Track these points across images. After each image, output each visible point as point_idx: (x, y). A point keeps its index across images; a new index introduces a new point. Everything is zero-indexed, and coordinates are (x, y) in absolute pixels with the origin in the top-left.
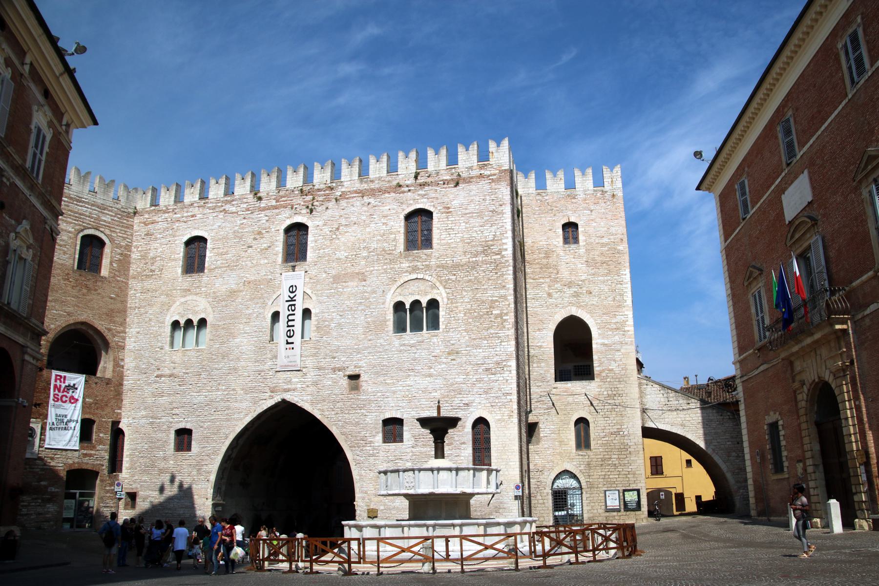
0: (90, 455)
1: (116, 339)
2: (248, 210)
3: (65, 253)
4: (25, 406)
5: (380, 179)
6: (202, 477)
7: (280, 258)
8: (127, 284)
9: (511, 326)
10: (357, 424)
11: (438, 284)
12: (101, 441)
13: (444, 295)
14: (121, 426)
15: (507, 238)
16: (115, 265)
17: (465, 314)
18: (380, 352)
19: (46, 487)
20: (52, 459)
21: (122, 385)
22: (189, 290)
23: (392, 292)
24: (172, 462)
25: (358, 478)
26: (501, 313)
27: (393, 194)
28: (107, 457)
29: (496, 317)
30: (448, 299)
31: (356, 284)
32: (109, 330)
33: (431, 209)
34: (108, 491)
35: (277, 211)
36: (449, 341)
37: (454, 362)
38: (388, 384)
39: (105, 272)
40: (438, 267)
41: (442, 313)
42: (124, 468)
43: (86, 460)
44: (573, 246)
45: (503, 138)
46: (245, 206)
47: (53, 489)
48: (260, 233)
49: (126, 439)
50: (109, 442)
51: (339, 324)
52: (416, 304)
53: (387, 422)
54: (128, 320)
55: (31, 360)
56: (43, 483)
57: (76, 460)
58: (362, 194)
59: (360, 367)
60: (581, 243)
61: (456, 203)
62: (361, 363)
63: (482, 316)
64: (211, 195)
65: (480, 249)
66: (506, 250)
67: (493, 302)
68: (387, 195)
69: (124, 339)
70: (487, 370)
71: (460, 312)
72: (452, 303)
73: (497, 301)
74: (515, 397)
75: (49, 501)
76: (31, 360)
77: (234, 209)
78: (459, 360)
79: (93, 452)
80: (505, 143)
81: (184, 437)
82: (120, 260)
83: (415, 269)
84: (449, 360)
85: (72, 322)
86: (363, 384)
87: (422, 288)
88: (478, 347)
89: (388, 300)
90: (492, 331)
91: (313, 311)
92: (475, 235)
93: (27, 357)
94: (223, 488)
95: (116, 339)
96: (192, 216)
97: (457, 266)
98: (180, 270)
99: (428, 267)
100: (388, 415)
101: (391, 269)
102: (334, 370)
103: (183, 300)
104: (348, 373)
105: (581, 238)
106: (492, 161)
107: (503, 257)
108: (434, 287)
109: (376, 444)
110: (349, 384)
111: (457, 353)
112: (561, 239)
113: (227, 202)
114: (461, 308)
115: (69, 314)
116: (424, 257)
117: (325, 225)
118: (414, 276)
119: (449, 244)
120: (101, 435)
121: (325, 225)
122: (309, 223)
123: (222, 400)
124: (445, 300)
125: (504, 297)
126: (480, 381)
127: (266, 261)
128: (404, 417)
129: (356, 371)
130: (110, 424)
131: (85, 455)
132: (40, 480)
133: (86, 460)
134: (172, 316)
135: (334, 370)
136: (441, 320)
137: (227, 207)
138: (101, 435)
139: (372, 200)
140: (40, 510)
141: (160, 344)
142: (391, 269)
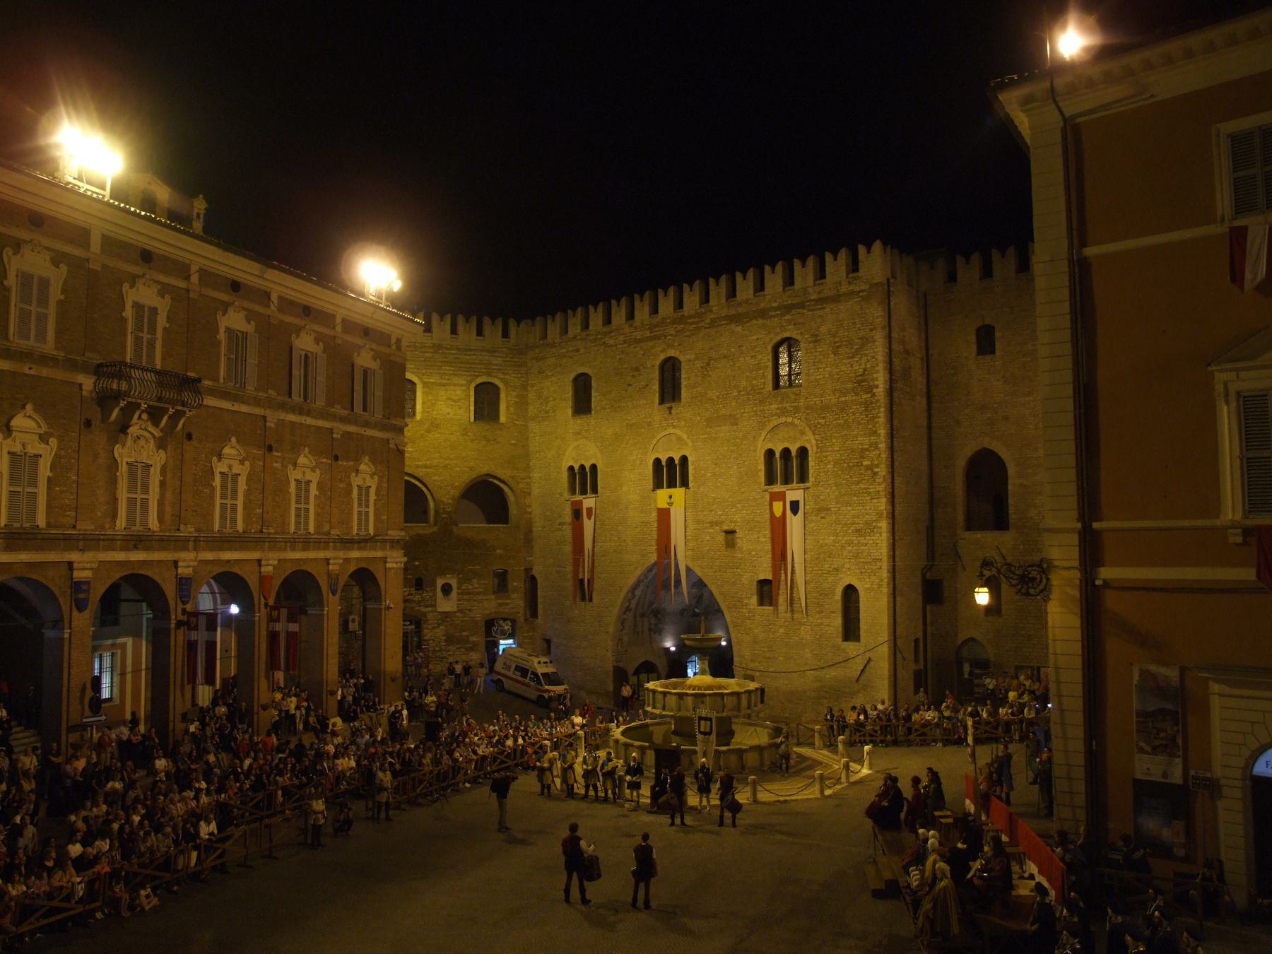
1: (521, 486)
2: (625, 342)
5: (747, 301)
7: (657, 401)
13: (814, 442)
14: (535, 572)
15: (877, 372)
21: (529, 531)
22: (579, 433)
27: (760, 321)
29: (868, 468)
32: (513, 478)
33: (798, 337)
35: (650, 344)
39: (503, 419)
40: (807, 408)
41: (812, 463)
44: (988, 357)
45: (873, 241)
46: (621, 338)
47: (473, 639)
48: (637, 369)
51: (714, 474)
52: (786, 452)
53: (763, 583)
58: (734, 319)
60: (998, 353)
61: (823, 329)
62: (736, 518)
64: (591, 323)
65: (850, 386)
66: (877, 387)
67: (863, 450)
68: (754, 322)
69: (529, 484)
73: (867, 450)
74: (885, 565)
75: (471, 649)
77: (612, 342)
80: (877, 246)
83: (784, 412)
86: (739, 541)
92: (844, 368)
95: (521, 486)
96: (578, 350)
98: (570, 412)
99: (797, 409)
100: (762, 577)
102: (712, 524)
103: (576, 444)
104: (725, 528)
105: (998, 346)
106: (862, 273)
107: (874, 395)
108: (803, 433)
110: (726, 539)
111: (828, 509)
112: (974, 348)
113: (606, 334)
116: (793, 397)
117: (696, 359)
118: (783, 419)
119: (817, 380)
121: (696, 359)
122: (681, 358)
125: (875, 446)
126: (850, 543)
129: (731, 528)
131: (500, 605)
135: (712, 524)
136: (811, 471)
137: (607, 340)
139: (739, 329)
140: (464, 657)
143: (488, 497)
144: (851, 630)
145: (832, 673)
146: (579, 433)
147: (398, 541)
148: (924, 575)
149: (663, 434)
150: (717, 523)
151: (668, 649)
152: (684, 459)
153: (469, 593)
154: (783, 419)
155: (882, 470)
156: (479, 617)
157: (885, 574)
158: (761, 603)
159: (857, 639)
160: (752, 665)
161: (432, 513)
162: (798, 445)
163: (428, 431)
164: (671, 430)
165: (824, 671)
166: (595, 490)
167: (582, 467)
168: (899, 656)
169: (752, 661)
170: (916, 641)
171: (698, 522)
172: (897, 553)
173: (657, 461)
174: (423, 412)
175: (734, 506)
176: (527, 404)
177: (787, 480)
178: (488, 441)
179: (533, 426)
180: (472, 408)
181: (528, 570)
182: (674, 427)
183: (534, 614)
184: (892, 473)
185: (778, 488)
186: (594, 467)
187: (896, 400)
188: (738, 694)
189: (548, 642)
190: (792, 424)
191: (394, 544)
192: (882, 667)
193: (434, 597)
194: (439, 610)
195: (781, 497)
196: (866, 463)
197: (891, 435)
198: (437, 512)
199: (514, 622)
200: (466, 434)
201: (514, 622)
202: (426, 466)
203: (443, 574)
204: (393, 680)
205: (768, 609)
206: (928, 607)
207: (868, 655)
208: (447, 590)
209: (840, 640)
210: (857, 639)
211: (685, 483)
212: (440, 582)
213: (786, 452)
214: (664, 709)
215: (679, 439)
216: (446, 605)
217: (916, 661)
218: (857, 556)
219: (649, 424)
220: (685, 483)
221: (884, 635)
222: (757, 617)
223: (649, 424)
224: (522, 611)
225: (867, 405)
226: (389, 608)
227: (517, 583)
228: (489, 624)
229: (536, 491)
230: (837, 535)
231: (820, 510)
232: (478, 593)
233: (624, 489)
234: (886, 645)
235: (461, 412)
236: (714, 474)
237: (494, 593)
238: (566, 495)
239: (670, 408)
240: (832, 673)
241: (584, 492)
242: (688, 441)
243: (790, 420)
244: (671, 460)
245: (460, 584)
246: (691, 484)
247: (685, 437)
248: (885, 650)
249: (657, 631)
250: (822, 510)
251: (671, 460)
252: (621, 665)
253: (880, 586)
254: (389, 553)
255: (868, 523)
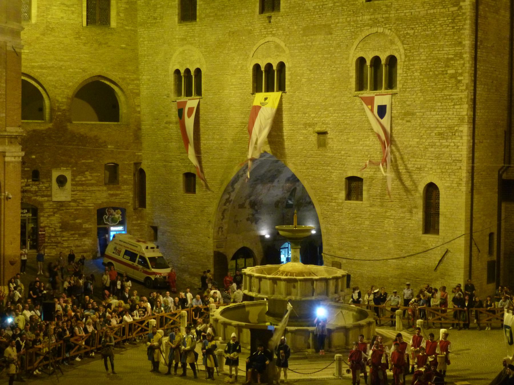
0: (116, 195)
1: (130, 87)
3: (73, 13)
4: (10, 198)
6: (205, 218)
7: (257, 10)
8: (136, 31)
9: (464, 88)
10: (325, 180)
11: (397, 39)
12: (125, 183)
13: (402, 51)
14: (144, 166)
16: (122, 15)
17: (421, 73)
18: (343, 110)
19: (81, 224)
20: (83, 200)
21: (140, 129)
23: (354, 47)
24: (182, 202)
25: (325, 231)
26: (456, 73)
28: (132, 195)
29: (453, 76)
30: (406, 56)
31: (323, 37)
32: (124, 79)
34: (135, 225)
36: (405, 102)
37: (409, 124)
38: (351, 143)
39: (113, 24)
40: (397, 19)
42: (147, 205)
43: (113, 199)
47: (86, 226)
49: (147, 178)
50: (132, 182)
52: (376, 60)
53: (351, 180)
54: (140, 67)
55: (13, 159)
56: (78, 221)
57: (105, 200)
59: (327, 124)
63: (437, 76)
67: (449, 60)
69: (138, 85)
70: (440, 134)
71: (416, 70)
72: (409, 60)
73: (452, 59)
75: (84, 235)
76: (13, 159)
78: (413, 122)
79: (119, 192)
81: (190, 180)
82: (126, 9)
83: (375, 23)
84: (404, 122)
85: (88, 77)
86: (330, 141)
87: (382, 43)
88: (433, 109)
89: (351, 55)
90: (446, 93)
91: (287, 65)
93: (7, 159)
94: (226, 227)
95: (130, 87)
97: (415, 19)
98: (176, 19)
100: (350, 174)
101: (354, 21)
102: (306, 125)
103: (181, 49)
104: (318, 129)
107: (461, 8)
108: (392, 43)
109: (340, 201)
110: (318, 140)
111: (413, 114)
114: (417, 67)
115: (84, 70)
116: (385, 9)
118: (375, 30)
120: (125, 177)
123: (217, 148)
124: (403, 57)
125: (460, 56)
127: (246, 11)
128: (364, 177)
130: (132, 168)
131: (112, 195)
132: (76, 218)
133: (113, 199)
134: (174, 65)
135: (306, 125)
136: (399, 78)
138: (125, 177)
140: (77, 243)
141: (166, 92)
142: (354, 21)
143: (100, 97)
144: (431, 225)
145: (412, 262)
146: (183, 39)
147: (16, 137)
148: (500, 176)
149: (262, 41)
150: (310, 125)
151: (263, 237)
152: (282, 65)
153: (82, 185)
154: (375, 30)
155: (466, 79)
156: (91, 207)
157: (464, 174)
158: (348, 197)
159: (436, 232)
160: (339, 253)
161: (47, 111)
162: (388, 54)
163: (43, 34)
164: (269, 38)
165: (405, 260)
166: (199, 92)
167: (188, 71)
168: (474, 249)
169: (340, 249)
170: (491, 235)
171: (293, 123)
172: (476, 155)
173: (257, 67)
174: (38, 16)
175: (326, 110)
176: (136, 10)
177: (376, 86)
178: (100, 44)
179: (141, 30)
180: (85, 13)
181: (137, 164)
182: (274, 35)
183: (143, 204)
184: (475, 82)
185: (367, 93)
186: (198, 71)
187: (481, 12)
188: (326, 280)
189: (155, 229)
190: (383, 34)
191: (12, 139)
192: (459, 258)
193: (49, 188)
194: (54, 199)
195: (370, 101)
196: (451, 71)
197: (476, 47)
198: (52, 110)
199: (124, 211)
200: (79, 38)
201: (124, 211)
202: (41, 67)
203: (57, 165)
204: (12, 263)
205: (353, 203)
206: (503, 205)
207: (446, 246)
208: (62, 181)
209: (421, 232)
210: (436, 232)
211: (282, 88)
212: (55, 174)
213: (376, 60)
214: (259, 292)
215: (277, 46)
216: (61, 195)
217: (490, 253)
218: (438, 157)
219: (250, 32)
220: (282, 88)
221: (462, 229)
222: (345, 210)
223: (250, 32)
224: (131, 201)
225: (454, 18)
226: (8, 198)
227: (127, 176)
228: (101, 213)
229: (144, 92)
230: (421, 137)
231: (407, 114)
232: (92, 185)
233: (226, 92)
234: (463, 239)
235: (74, 16)
236: (309, 80)
237: (106, 184)
238: (173, 97)
239: (270, 17)
240: (412, 262)
241: (189, 94)
242: (286, 49)
243: (381, 30)
244: (269, 66)
245: (74, 176)
246: (287, 89)
247: (282, 44)
248: (461, 243)
249: (254, 220)
250: (408, 115)
251: (269, 66)
252: (221, 250)
253: (459, 184)
254: (7, 148)
255: (450, 128)
